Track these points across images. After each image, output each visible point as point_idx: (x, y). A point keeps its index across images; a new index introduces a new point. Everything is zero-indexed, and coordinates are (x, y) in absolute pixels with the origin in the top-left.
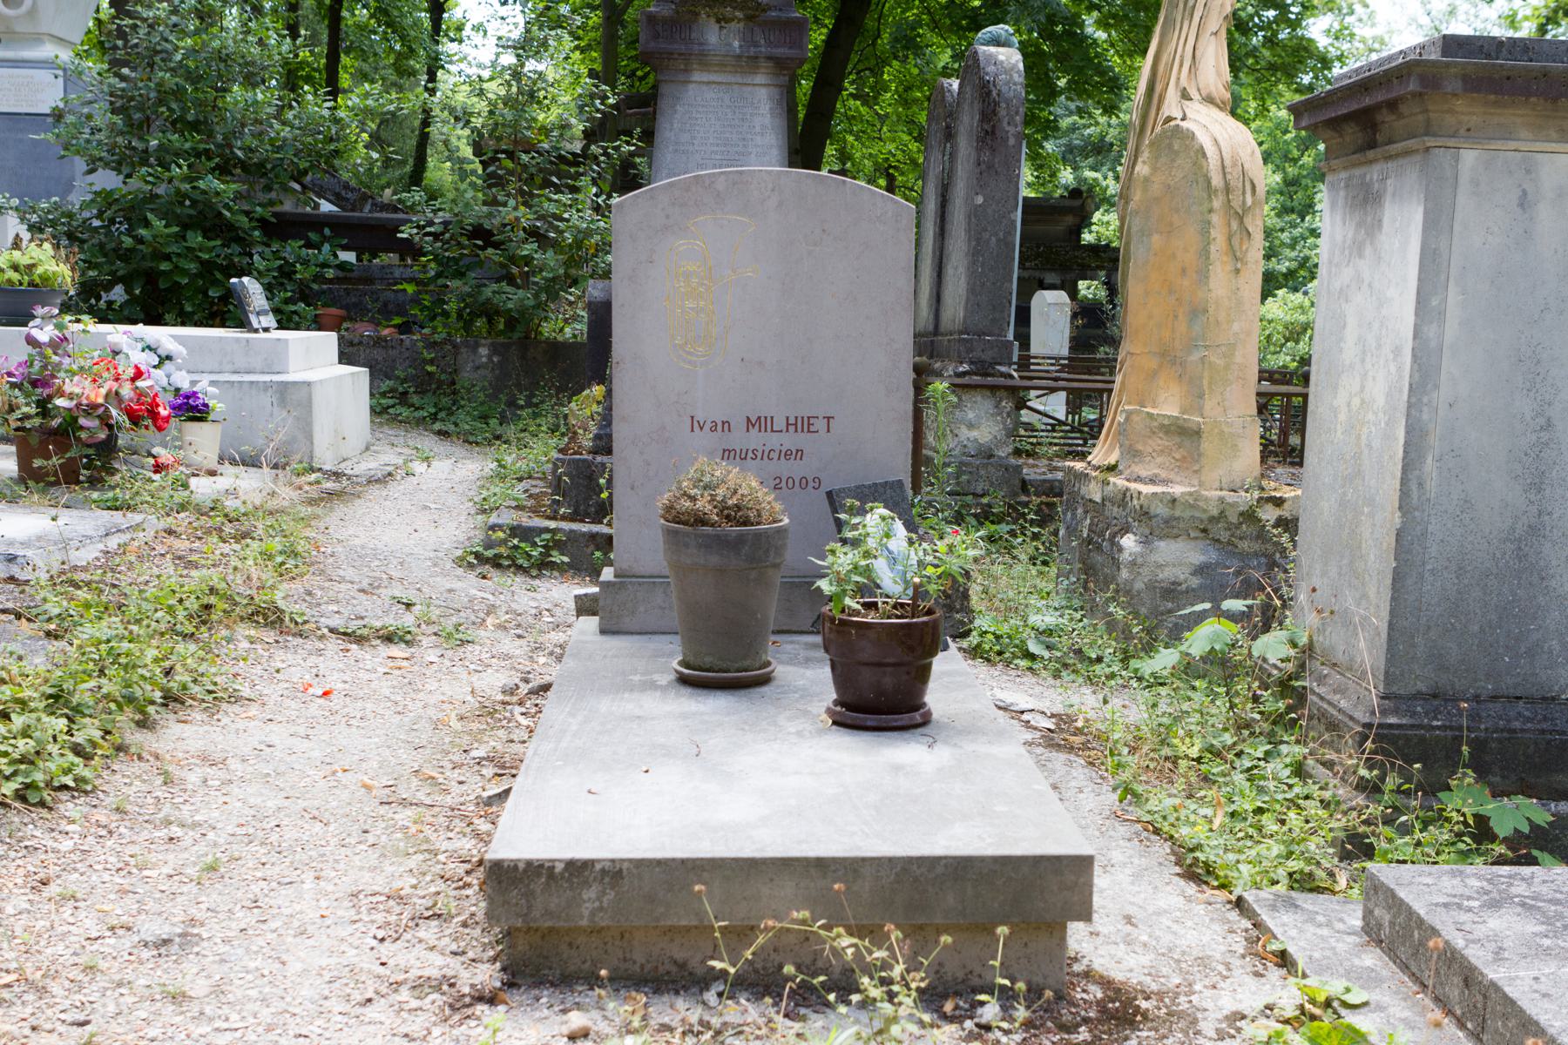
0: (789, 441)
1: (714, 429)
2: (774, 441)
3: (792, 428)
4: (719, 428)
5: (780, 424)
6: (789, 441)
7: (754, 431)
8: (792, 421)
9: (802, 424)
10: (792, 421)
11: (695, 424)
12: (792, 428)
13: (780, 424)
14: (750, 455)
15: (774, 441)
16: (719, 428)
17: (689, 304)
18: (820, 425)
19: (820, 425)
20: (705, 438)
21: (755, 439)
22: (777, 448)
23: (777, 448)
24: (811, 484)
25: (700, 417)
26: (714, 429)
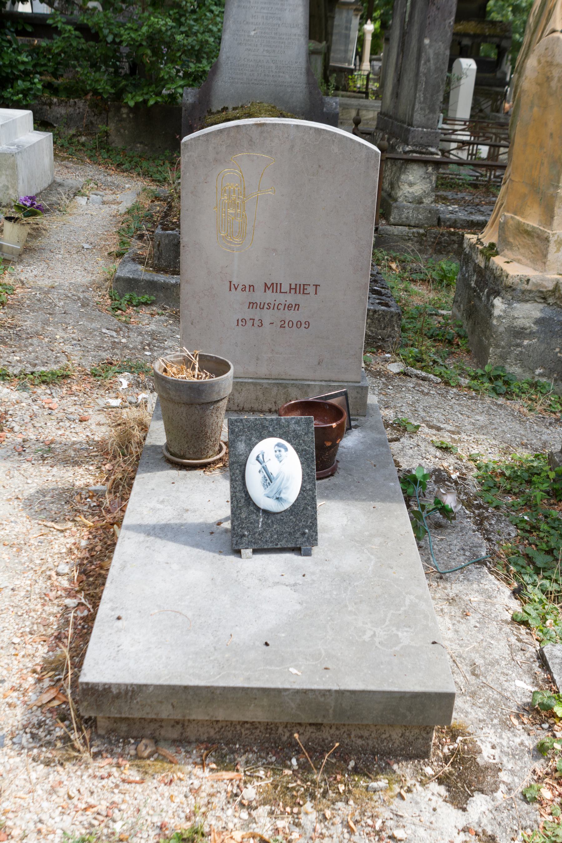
0: (290, 299)
1: (244, 290)
2: (281, 298)
3: (293, 291)
4: (247, 289)
5: (285, 288)
6: (290, 299)
7: (269, 292)
8: (293, 286)
9: (300, 289)
10: (293, 286)
11: (232, 286)
12: (293, 291)
13: (285, 288)
14: (266, 306)
15: (281, 298)
16: (247, 289)
17: (231, 211)
18: (311, 290)
19: (311, 290)
20: (239, 296)
21: (270, 297)
22: (283, 302)
23: (283, 302)
24: (303, 325)
25: (235, 281)
26: (244, 290)
